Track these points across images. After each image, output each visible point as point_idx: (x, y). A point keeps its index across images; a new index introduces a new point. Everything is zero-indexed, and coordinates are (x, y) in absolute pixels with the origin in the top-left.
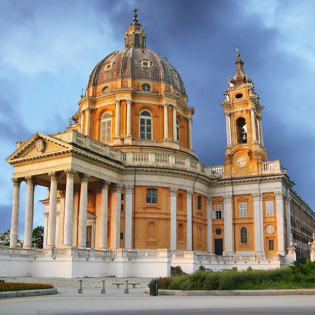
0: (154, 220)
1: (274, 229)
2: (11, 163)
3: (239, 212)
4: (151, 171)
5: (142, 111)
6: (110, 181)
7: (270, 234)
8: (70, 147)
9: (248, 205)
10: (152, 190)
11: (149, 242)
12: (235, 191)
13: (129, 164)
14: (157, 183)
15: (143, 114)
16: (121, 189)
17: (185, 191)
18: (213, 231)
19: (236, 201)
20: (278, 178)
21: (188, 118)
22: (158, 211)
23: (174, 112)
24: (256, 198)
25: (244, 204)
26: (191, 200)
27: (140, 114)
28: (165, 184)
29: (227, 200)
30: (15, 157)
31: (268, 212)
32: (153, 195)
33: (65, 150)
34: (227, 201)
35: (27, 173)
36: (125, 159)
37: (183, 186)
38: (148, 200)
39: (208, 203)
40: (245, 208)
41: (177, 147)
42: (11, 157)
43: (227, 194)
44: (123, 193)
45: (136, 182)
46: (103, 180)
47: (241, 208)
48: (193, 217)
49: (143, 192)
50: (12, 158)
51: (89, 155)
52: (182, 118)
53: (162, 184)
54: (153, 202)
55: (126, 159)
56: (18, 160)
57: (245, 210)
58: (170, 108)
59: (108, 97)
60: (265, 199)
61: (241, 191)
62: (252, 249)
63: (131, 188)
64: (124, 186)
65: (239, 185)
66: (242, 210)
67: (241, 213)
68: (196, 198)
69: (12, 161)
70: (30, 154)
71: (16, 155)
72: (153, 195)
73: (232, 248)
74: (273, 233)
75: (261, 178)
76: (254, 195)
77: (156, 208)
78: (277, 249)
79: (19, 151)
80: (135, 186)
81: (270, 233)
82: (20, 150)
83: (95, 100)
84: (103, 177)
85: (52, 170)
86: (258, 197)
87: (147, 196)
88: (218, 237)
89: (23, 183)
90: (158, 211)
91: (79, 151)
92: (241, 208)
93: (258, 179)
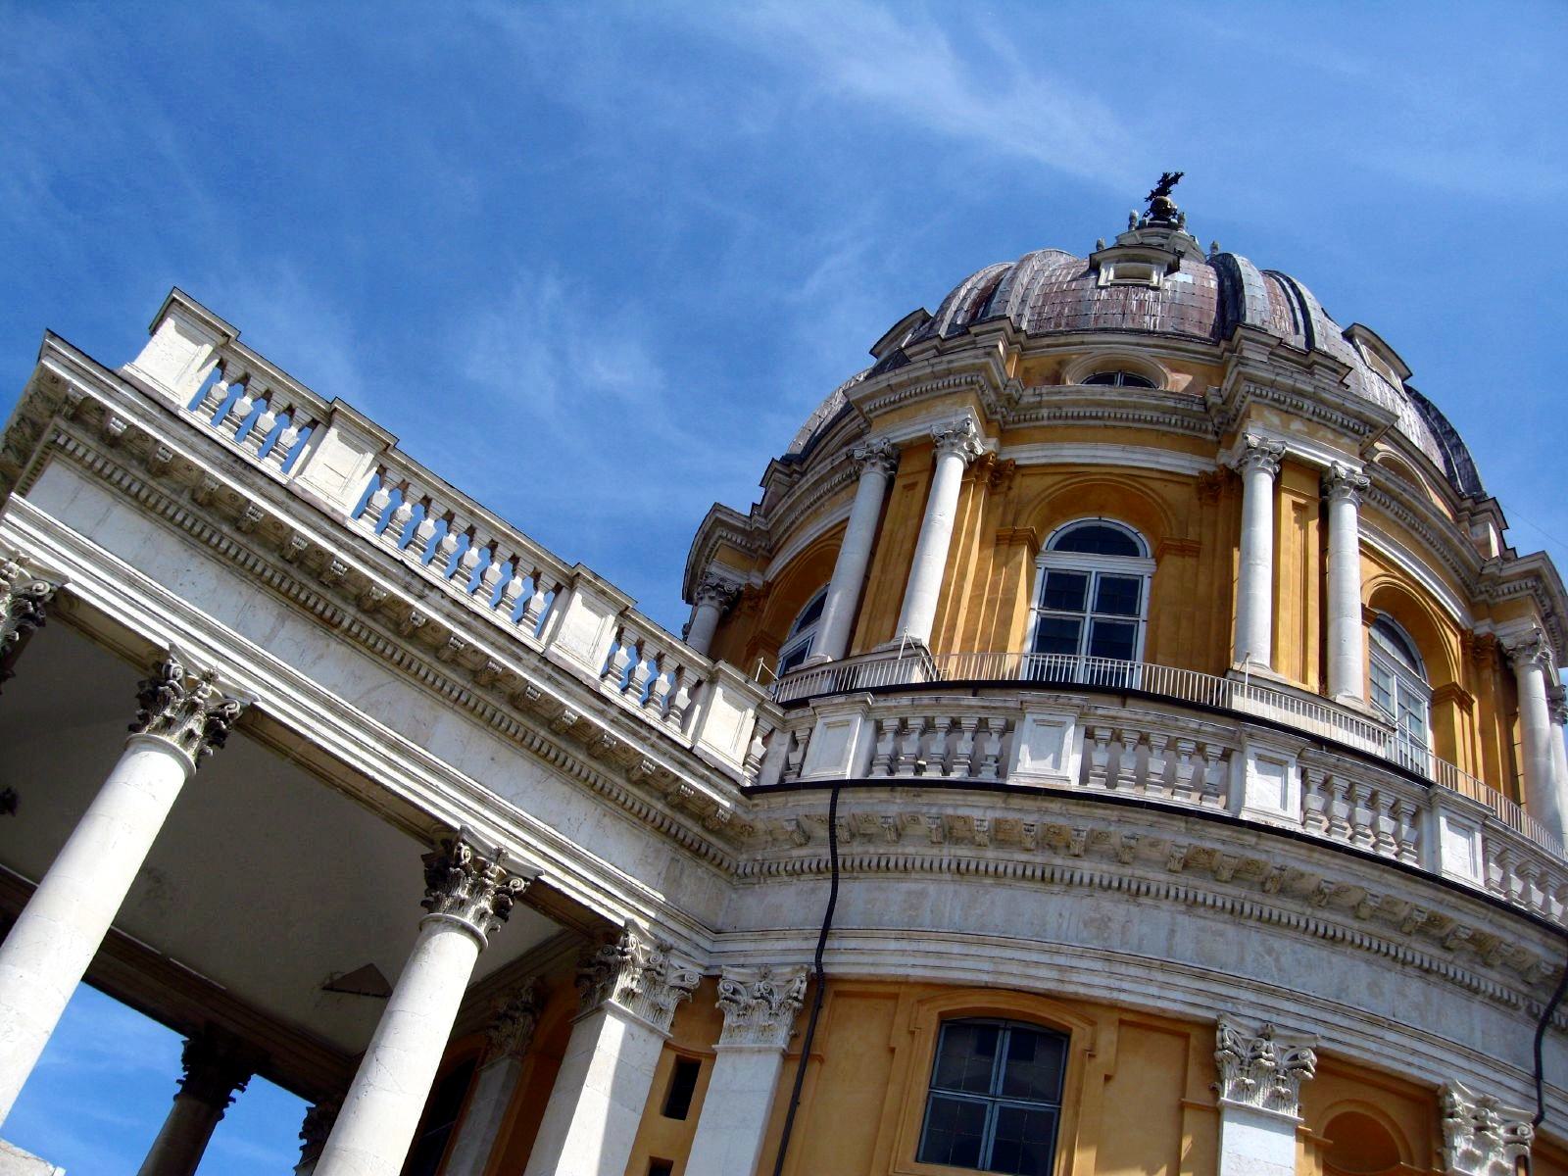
4: (1001, 836)
5: (1066, 526)
10: (1004, 1043)
14: (1061, 960)
15: (1067, 544)
16: (670, 1002)
21: (1508, 643)
27: (1049, 539)
32: (1012, 1088)
37: (1391, 1036)
44: (694, 1046)
45: (828, 944)
49: (901, 1041)
52: (1454, 642)
59: (837, 478)
63: (776, 999)
64: (712, 980)
72: (1012, 1088)
80: (820, 983)
87: (947, 1093)
91: (130, 408)
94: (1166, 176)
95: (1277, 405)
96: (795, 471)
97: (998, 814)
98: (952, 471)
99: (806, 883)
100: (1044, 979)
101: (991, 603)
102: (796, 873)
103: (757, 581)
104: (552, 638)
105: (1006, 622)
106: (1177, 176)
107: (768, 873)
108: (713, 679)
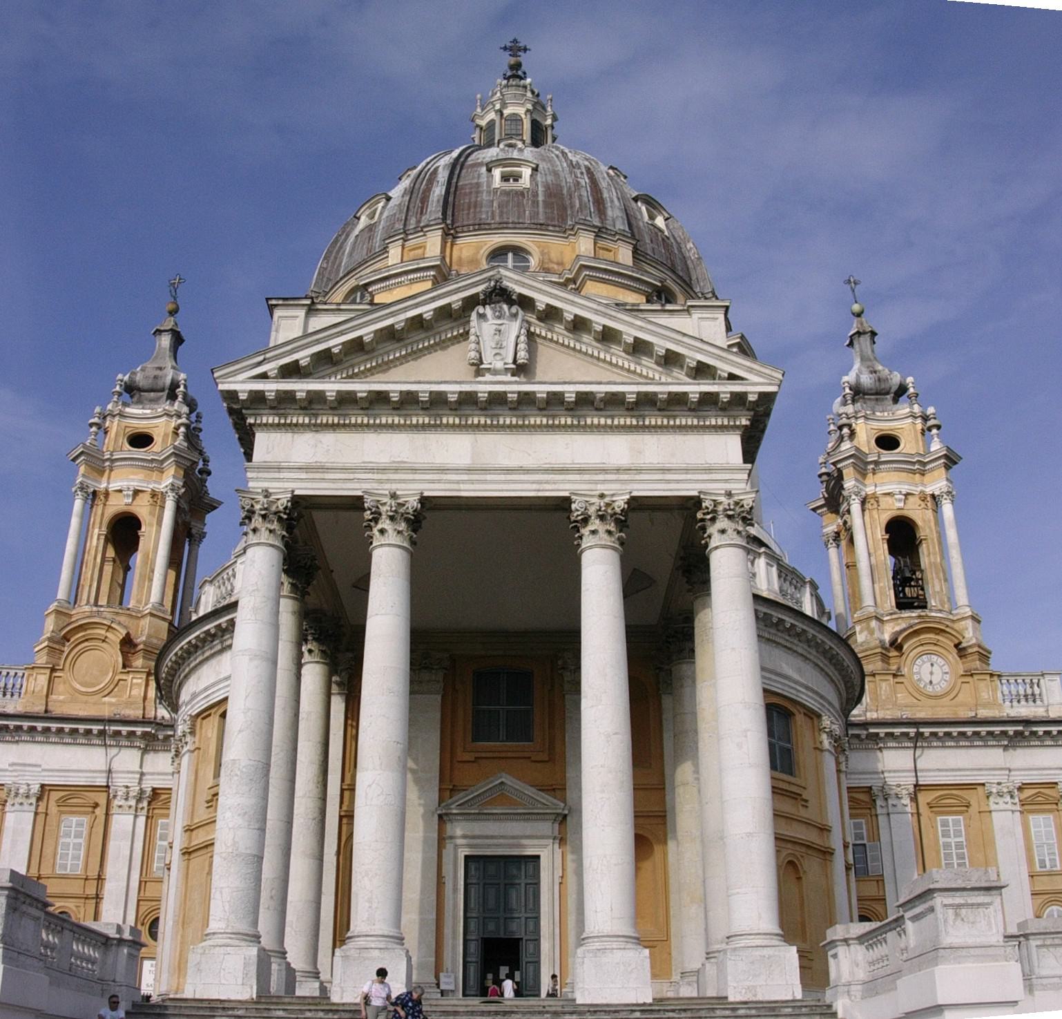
3: (938, 852)
8: (759, 374)
9: (967, 827)
12: (922, 771)
19: (924, 810)
22: (803, 813)
24: (1001, 801)
25: (956, 823)
30: (292, 371)
33: (725, 390)
35: (376, 476)
40: (961, 836)
42: (259, 364)
47: (943, 836)
56: (331, 386)
57: (959, 846)
60: (1027, 807)
61: (947, 770)
66: (947, 846)
67: (949, 856)
69: (271, 388)
70: (397, 373)
71: (303, 356)
76: (994, 790)
79: (335, 344)
82: (342, 333)
85: (597, 482)
86: (1008, 799)
92: (943, 836)
94: (515, 41)
96: (452, 234)
100: (791, 694)
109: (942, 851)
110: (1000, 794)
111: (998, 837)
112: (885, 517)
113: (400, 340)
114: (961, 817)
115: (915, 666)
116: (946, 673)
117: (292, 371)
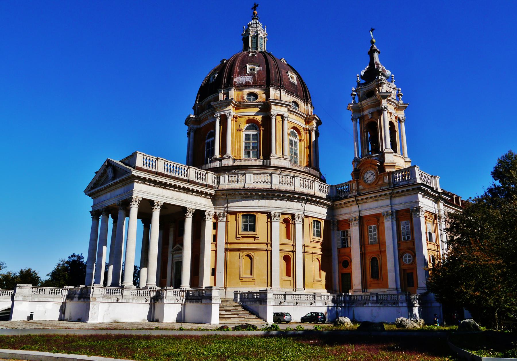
0: (251, 252)
1: (412, 258)
2: (90, 195)
6: (194, 208)
7: (408, 265)
11: (245, 278)
13: (222, 187)
14: (254, 208)
17: (293, 215)
18: (339, 263)
20: (413, 189)
21: (310, 129)
23: (286, 122)
26: (301, 225)
28: (264, 208)
29: (353, 223)
30: (92, 188)
31: (403, 236)
34: (354, 224)
36: (218, 183)
37: (289, 210)
38: (245, 229)
39: (332, 228)
41: (286, 164)
42: (88, 189)
43: (353, 215)
46: (186, 208)
48: (304, 246)
50: (89, 189)
51: (159, 179)
53: (260, 208)
54: (250, 231)
55: (219, 181)
57: (374, 235)
58: (279, 118)
59: (210, 113)
62: (386, 286)
64: (216, 213)
65: (367, 202)
67: (371, 239)
68: (310, 223)
69: (89, 193)
73: (361, 284)
74: (412, 264)
75: (391, 192)
77: (254, 237)
78: (418, 286)
81: (408, 263)
83: (199, 118)
84: (184, 203)
88: (346, 271)
89: (100, 217)
90: (256, 241)
92: (370, 232)
93: (387, 193)
94: (255, 4)
95: (275, 105)
97: (245, 192)
98: (229, 120)
99: (224, 200)
101: (238, 142)
102: (222, 199)
103: (198, 126)
104: (189, 177)
105: (240, 146)
106: (258, 5)
107: (219, 198)
108: (207, 173)
109: (369, 237)
110: (388, 215)
111: (386, 231)
112: (366, 123)
113: (103, 177)
114: (376, 225)
115: (365, 176)
116: (374, 176)
117: (92, 188)
